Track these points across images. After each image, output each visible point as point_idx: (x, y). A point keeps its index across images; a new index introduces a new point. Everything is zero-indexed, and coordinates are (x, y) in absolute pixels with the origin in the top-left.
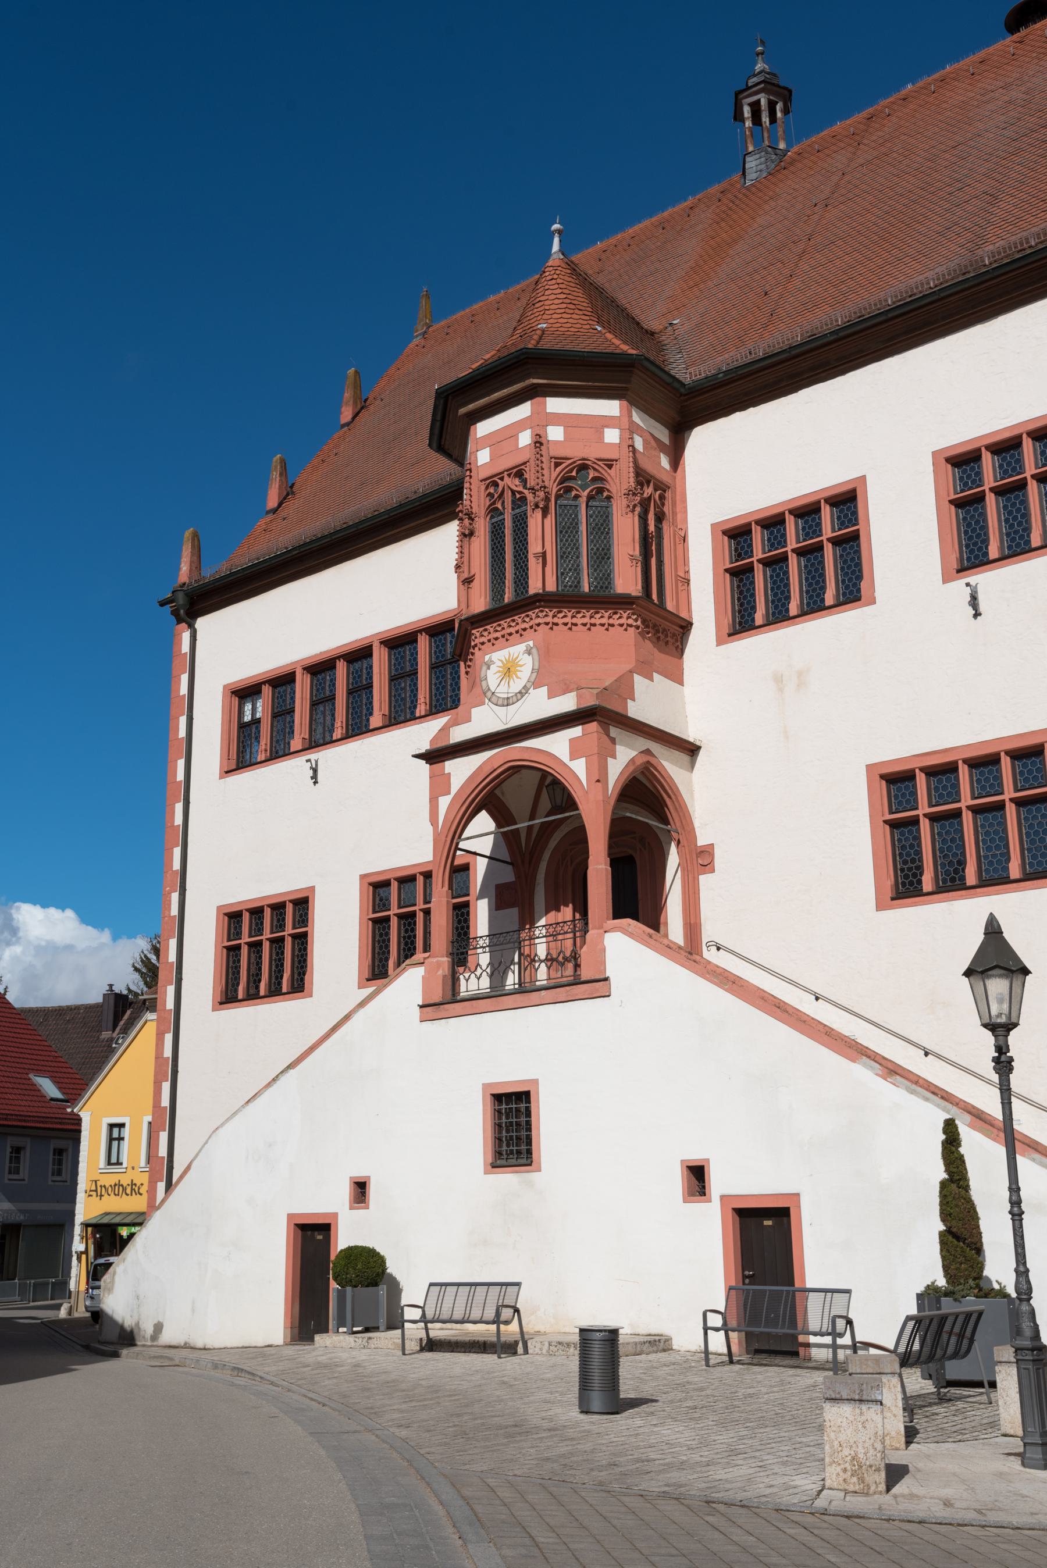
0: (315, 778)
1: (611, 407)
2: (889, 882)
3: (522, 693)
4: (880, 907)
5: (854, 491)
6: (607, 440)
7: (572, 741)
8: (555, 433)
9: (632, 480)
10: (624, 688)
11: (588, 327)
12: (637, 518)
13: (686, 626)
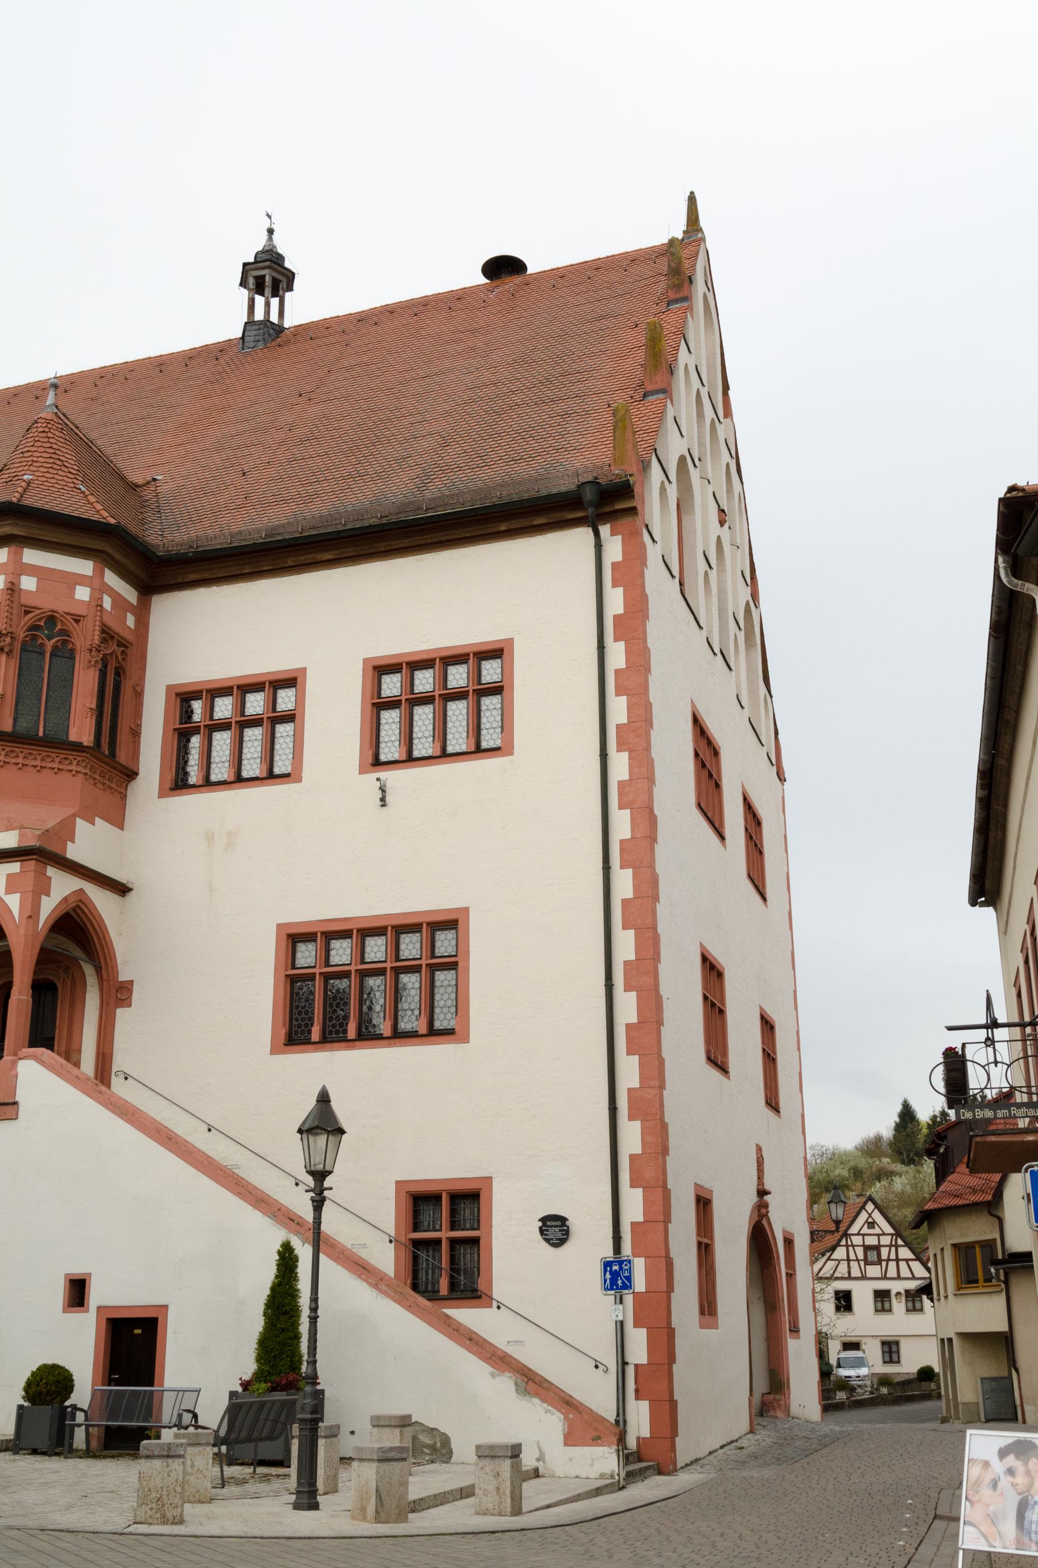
1: (84, 567)
2: (283, 1032)
4: (274, 1051)
5: (295, 679)
6: (77, 597)
7: (10, 876)
8: (28, 583)
9: (96, 637)
10: (66, 831)
11: (72, 485)
12: (97, 673)
13: (131, 775)
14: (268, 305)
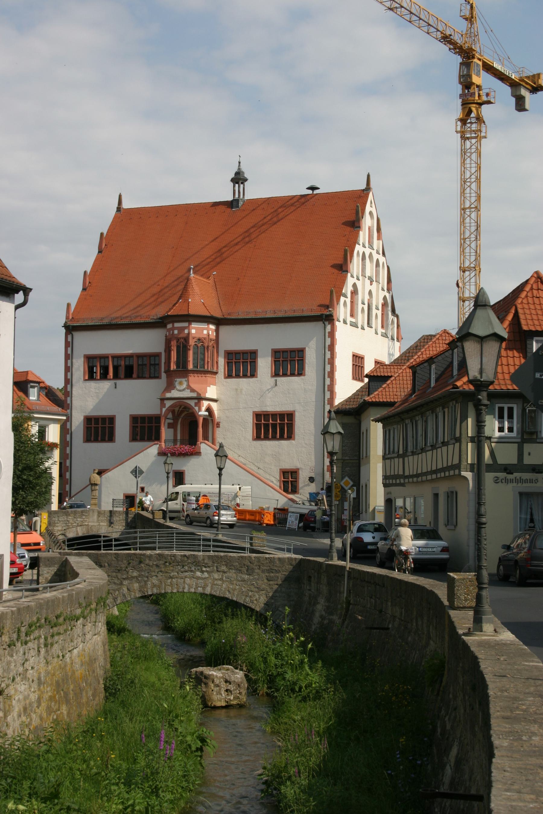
0: (116, 387)
3: (184, 390)
14: (239, 187)
